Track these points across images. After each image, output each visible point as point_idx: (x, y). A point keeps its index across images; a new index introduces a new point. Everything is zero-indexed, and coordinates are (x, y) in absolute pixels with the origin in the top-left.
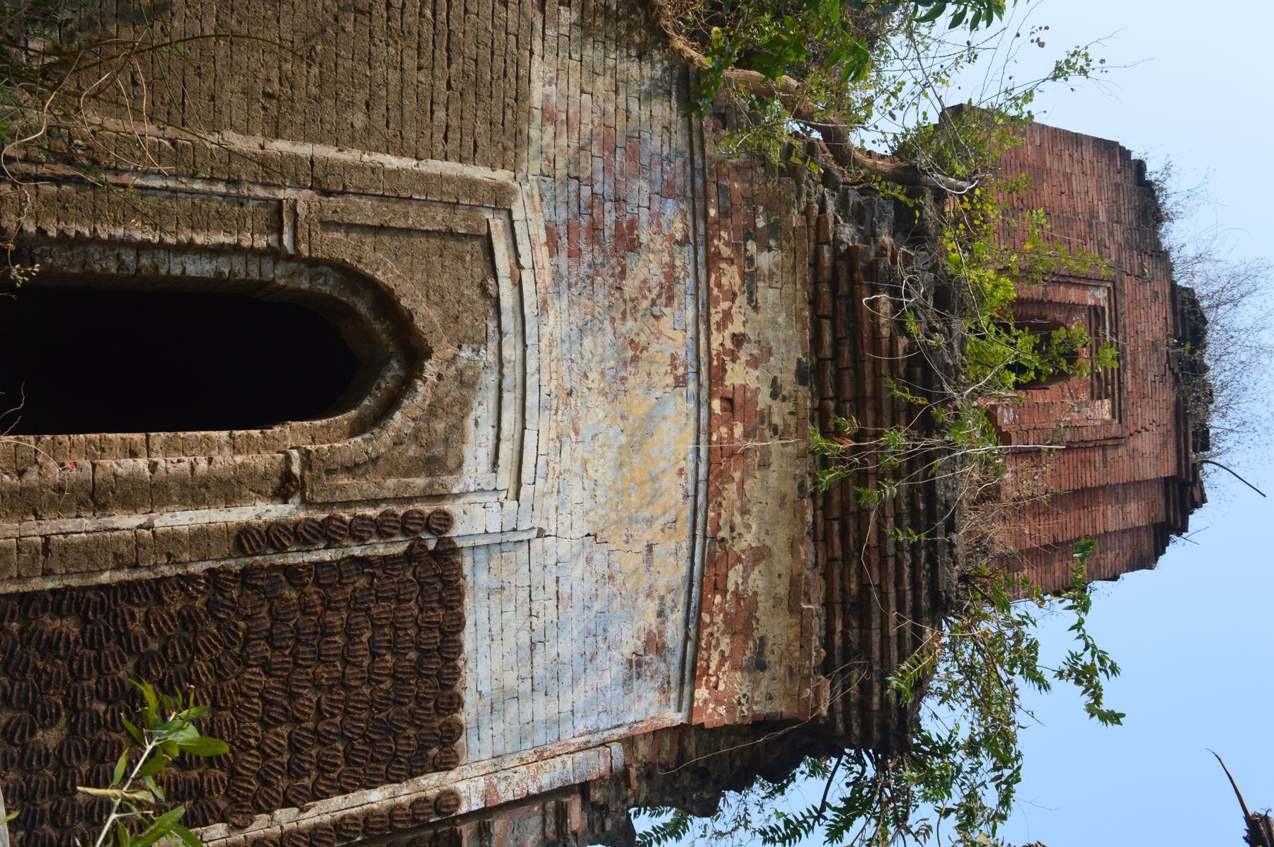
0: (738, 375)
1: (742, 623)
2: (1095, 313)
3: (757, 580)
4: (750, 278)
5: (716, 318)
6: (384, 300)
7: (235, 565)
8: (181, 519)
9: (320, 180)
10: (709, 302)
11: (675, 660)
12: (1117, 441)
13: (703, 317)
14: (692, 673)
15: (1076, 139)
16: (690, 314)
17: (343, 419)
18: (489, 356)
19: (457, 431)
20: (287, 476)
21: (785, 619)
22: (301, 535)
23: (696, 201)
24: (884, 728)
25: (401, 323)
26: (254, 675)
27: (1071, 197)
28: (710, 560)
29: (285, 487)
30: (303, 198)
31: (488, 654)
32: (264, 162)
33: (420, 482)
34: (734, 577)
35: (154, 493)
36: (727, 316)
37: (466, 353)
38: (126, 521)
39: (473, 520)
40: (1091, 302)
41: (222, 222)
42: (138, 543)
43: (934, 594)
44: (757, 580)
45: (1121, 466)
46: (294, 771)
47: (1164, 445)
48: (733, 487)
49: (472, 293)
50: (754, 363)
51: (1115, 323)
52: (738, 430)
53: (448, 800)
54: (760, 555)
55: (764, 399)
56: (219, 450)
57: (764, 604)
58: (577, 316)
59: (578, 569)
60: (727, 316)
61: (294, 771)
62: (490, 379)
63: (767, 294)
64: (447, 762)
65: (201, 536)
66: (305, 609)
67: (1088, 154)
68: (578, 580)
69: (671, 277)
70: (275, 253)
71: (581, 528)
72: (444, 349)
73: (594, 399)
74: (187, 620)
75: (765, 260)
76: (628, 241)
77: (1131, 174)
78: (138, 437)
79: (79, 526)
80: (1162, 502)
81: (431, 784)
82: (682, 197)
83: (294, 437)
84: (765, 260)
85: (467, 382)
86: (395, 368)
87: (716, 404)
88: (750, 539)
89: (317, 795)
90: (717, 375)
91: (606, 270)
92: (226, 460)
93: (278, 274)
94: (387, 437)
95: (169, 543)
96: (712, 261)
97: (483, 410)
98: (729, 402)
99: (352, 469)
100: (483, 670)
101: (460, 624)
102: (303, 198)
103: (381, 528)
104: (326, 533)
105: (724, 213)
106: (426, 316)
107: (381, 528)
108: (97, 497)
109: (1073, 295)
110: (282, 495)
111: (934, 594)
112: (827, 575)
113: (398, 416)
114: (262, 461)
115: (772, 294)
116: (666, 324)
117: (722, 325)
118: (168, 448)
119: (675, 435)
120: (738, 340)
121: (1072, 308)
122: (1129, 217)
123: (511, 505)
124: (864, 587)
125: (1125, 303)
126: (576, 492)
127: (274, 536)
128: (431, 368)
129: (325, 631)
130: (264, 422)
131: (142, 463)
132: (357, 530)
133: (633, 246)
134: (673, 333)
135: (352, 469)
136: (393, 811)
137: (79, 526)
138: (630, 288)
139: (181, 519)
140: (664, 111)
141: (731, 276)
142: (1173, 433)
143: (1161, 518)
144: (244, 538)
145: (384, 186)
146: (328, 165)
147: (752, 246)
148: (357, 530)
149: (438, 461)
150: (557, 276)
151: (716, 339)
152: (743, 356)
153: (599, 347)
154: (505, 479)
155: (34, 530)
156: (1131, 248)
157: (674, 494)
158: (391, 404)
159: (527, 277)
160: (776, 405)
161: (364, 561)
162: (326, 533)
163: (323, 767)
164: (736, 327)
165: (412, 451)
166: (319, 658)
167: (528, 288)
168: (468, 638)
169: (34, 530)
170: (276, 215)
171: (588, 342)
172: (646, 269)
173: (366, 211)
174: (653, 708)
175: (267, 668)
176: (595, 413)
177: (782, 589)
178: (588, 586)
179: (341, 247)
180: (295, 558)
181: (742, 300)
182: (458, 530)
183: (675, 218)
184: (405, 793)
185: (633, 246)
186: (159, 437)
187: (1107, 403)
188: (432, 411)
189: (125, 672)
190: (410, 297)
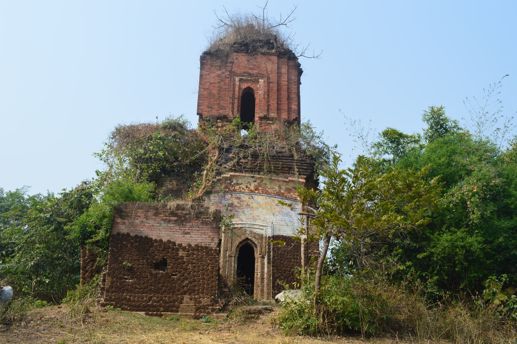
0: (252, 188)
1: (289, 190)
2: (241, 80)
3: (283, 187)
4: (237, 184)
5: (243, 191)
6: (240, 243)
7: (272, 264)
8: (266, 270)
9: (226, 251)
10: (241, 191)
11: (293, 202)
12: (269, 78)
13: (243, 193)
14: (295, 200)
15: (201, 76)
16: (242, 195)
17: (255, 249)
18: (248, 229)
19: (258, 234)
20: (262, 257)
21: (290, 184)
22: (269, 256)
23: (225, 192)
24: (310, 167)
25: (243, 241)
26: (285, 263)
27: (214, 83)
28: (279, 195)
29: (263, 257)
30: (228, 253)
31: (288, 232)
32: (224, 258)
33: (264, 240)
34: (282, 191)
35: (262, 273)
36: (243, 189)
37: (248, 232)
38: (265, 276)
39: (269, 233)
40: (238, 83)
41: (231, 263)
42: (268, 275)
43: (290, 157)
44: (283, 187)
45: (274, 77)
46: (297, 259)
47: (270, 60)
48: (269, 190)
49: (240, 231)
50: (250, 185)
51: (243, 76)
52: (260, 188)
53: (305, 240)
54: (280, 187)
55: (256, 184)
56: (258, 265)
57: (287, 187)
58: (243, 214)
59: (278, 217)
60: (243, 189)
61: (297, 259)
62: (251, 229)
63: (240, 181)
64: (300, 240)
65: (268, 268)
66: (278, 256)
67: (204, 73)
68: (279, 217)
69: (237, 198)
70: (234, 256)
71: (272, 216)
72: (247, 236)
73: (254, 213)
74: (277, 270)
75: (235, 181)
76: (231, 205)
77: (208, 57)
78: (256, 274)
79: (266, 281)
80: (283, 59)
81: (302, 242)
82: (225, 195)
83: (257, 255)
84: (235, 181)
85: (251, 232)
86: (249, 241)
87: (256, 192)
88: (277, 188)
89: (301, 257)
90: (252, 191)
91: (236, 209)
92: (259, 264)
93: (237, 256)
94: (258, 244)
95: (268, 271)
96: (235, 190)
97: (255, 231)
98: (256, 189)
99: (262, 249)
100: (289, 233)
101: (283, 236)
102: (228, 253)
103: (269, 246)
104: (269, 252)
105: (227, 188)
106: (243, 238)
107: (269, 246)
108: (262, 279)
109: (237, 89)
110: (264, 258)
111: (290, 157)
112: (284, 173)
113: (256, 243)
114: (260, 260)
115: (240, 181)
116: (244, 199)
117: (245, 190)
118: (257, 270)
119: (260, 199)
120: (247, 187)
121: (240, 88)
122: (218, 63)
123: (268, 227)
124: (287, 167)
125: (238, 71)
126: (267, 217)
127: (269, 259)
128: (250, 238)
129: (281, 254)
130: (254, 259)
131: (259, 274)
132: (269, 249)
133: (232, 204)
134: (245, 198)
135: (262, 249)
136: (305, 247)
137: (266, 281)
138: (239, 205)
139: (266, 270)
140: (212, 197)
141: (237, 187)
142: (268, 56)
143: (286, 60)
144: (269, 263)
145: (226, 242)
146: (224, 250)
147: (232, 183)
148: (269, 249)
149: (261, 237)
150: (238, 217)
151: (246, 191)
152: (249, 186)
153: (247, 211)
154: (264, 228)
155: (265, 285)
156: (226, 66)
157: (269, 200)
158: (254, 243)
159: (238, 223)
160: (257, 181)
161: (273, 248)
162: (269, 252)
163: (297, 255)
164: (245, 187)
165: (260, 241)
166: (284, 255)
167: (239, 223)
168: (285, 235)
169: (265, 285)
170: (230, 256)
171: (246, 213)
172: (236, 202)
173: (229, 245)
174: (299, 207)
175: (284, 261)
176: (256, 213)
177: (285, 184)
178: (280, 216)
179: (234, 249)
180: (272, 257)
181: (241, 186)
182: (271, 236)
183: (228, 196)
184: (302, 246)
185: (232, 204)
186: (256, 271)
187: (260, 80)
188: (255, 238)
189: (282, 277)
190: (240, 240)
